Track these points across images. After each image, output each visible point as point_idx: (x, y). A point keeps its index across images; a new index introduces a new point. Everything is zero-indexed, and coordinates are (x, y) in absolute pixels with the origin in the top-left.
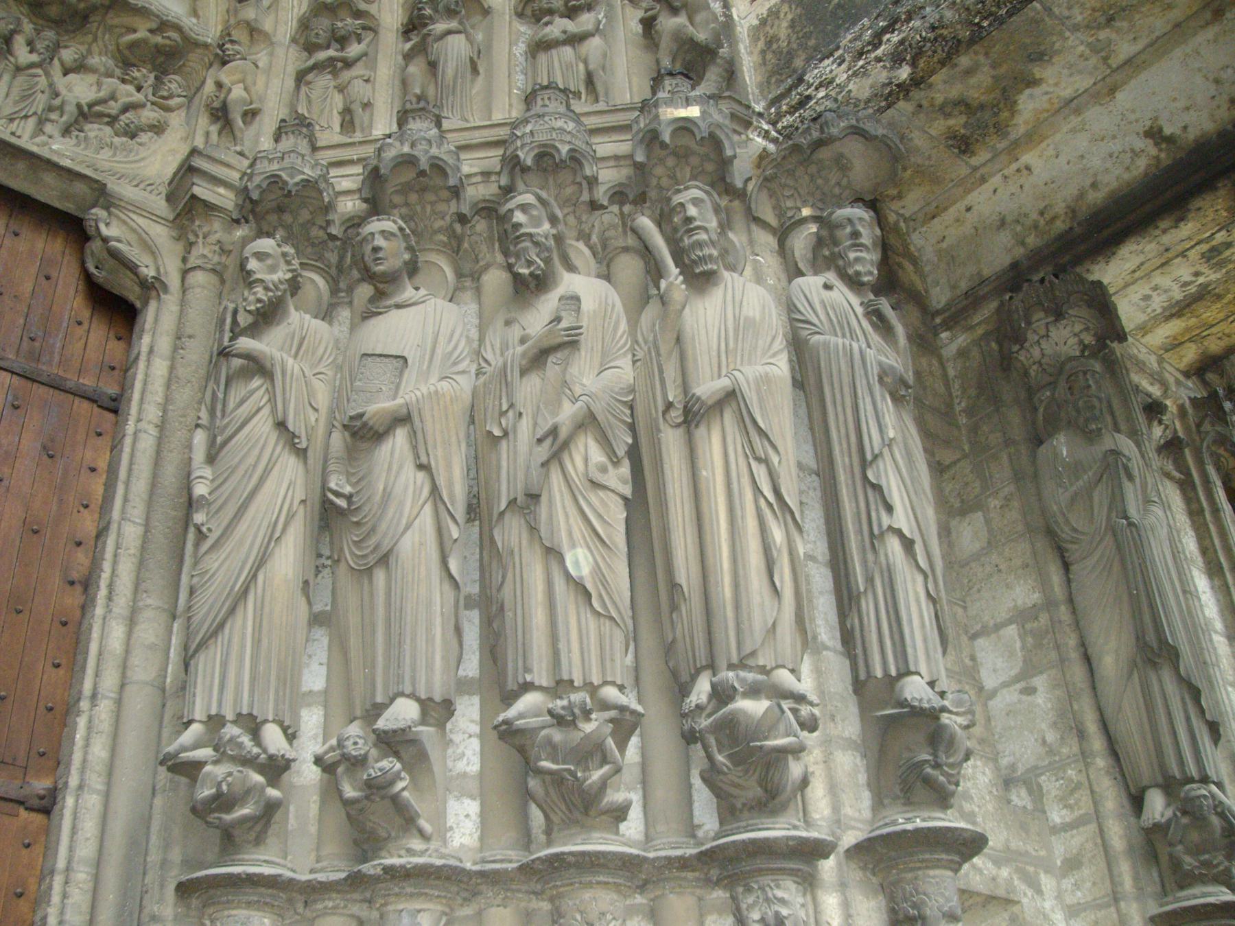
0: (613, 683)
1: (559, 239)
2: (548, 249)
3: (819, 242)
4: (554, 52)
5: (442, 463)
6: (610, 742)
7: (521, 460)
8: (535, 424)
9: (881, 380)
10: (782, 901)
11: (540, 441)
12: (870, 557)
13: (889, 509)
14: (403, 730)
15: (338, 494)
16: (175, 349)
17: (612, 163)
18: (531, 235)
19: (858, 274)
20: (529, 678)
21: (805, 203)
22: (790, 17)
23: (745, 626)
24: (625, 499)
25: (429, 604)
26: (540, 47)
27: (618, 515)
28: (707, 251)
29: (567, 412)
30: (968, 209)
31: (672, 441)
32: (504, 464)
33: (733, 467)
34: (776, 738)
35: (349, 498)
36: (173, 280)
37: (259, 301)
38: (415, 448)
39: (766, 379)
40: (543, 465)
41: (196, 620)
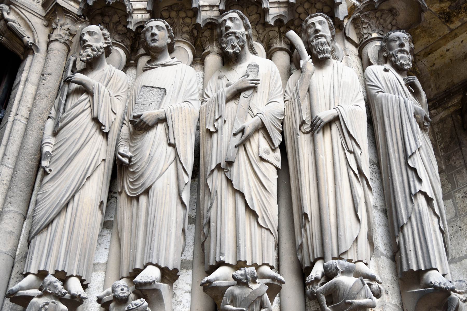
0: (268, 265)
2: (243, 41)
3: (382, 49)
5: (181, 144)
6: (266, 296)
7: (225, 144)
8: (233, 126)
11: (235, 135)
14: (150, 283)
15: (123, 156)
16: (40, 80)
18: (234, 33)
19: (402, 64)
20: (222, 259)
21: (374, 31)
23: (342, 237)
24: (277, 168)
25: (169, 216)
27: (274, 176)
28: (325, 47)
29: (250, 123)
30: (448, 50)
31: (304, 141)
32: (215, 145)
34: (359, 298)
35: (130, 159)
36: (42, 46)
37: (88, 55)
38: (167, 135)
40: (236, 147)
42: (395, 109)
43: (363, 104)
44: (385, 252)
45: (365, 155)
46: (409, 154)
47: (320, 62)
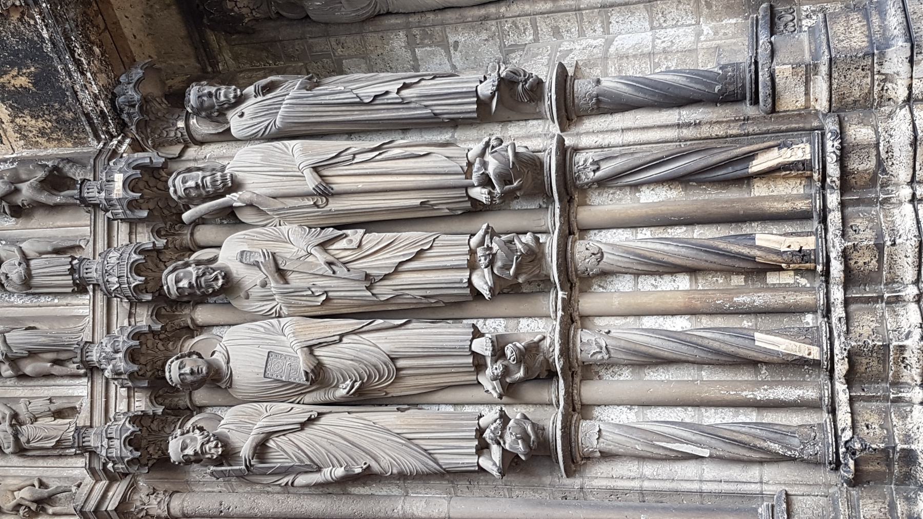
1: (198, 263)
3: (209, 117)
4: (33, 272)
9: (310, 90)
10: (585, 161)
11: (334, 272)
12: (412, 105)
13: (387, 93)
17: (134, 236)
18: (198, 278)
19: (235, 97)
21: (174, 125)
22: (29, 118)
23: (447, 170)
24: (365, 233)
26: (27, 285)
27: (374, 235)
31: (335, 205)
33: (356, 172)
39: (304, 151)
41: (420, 467)
42: (307, 109)
43: (275, 143)
44: (450, 135)
45: (356, 145)
46: (358, 100)
47: (236, 186)
